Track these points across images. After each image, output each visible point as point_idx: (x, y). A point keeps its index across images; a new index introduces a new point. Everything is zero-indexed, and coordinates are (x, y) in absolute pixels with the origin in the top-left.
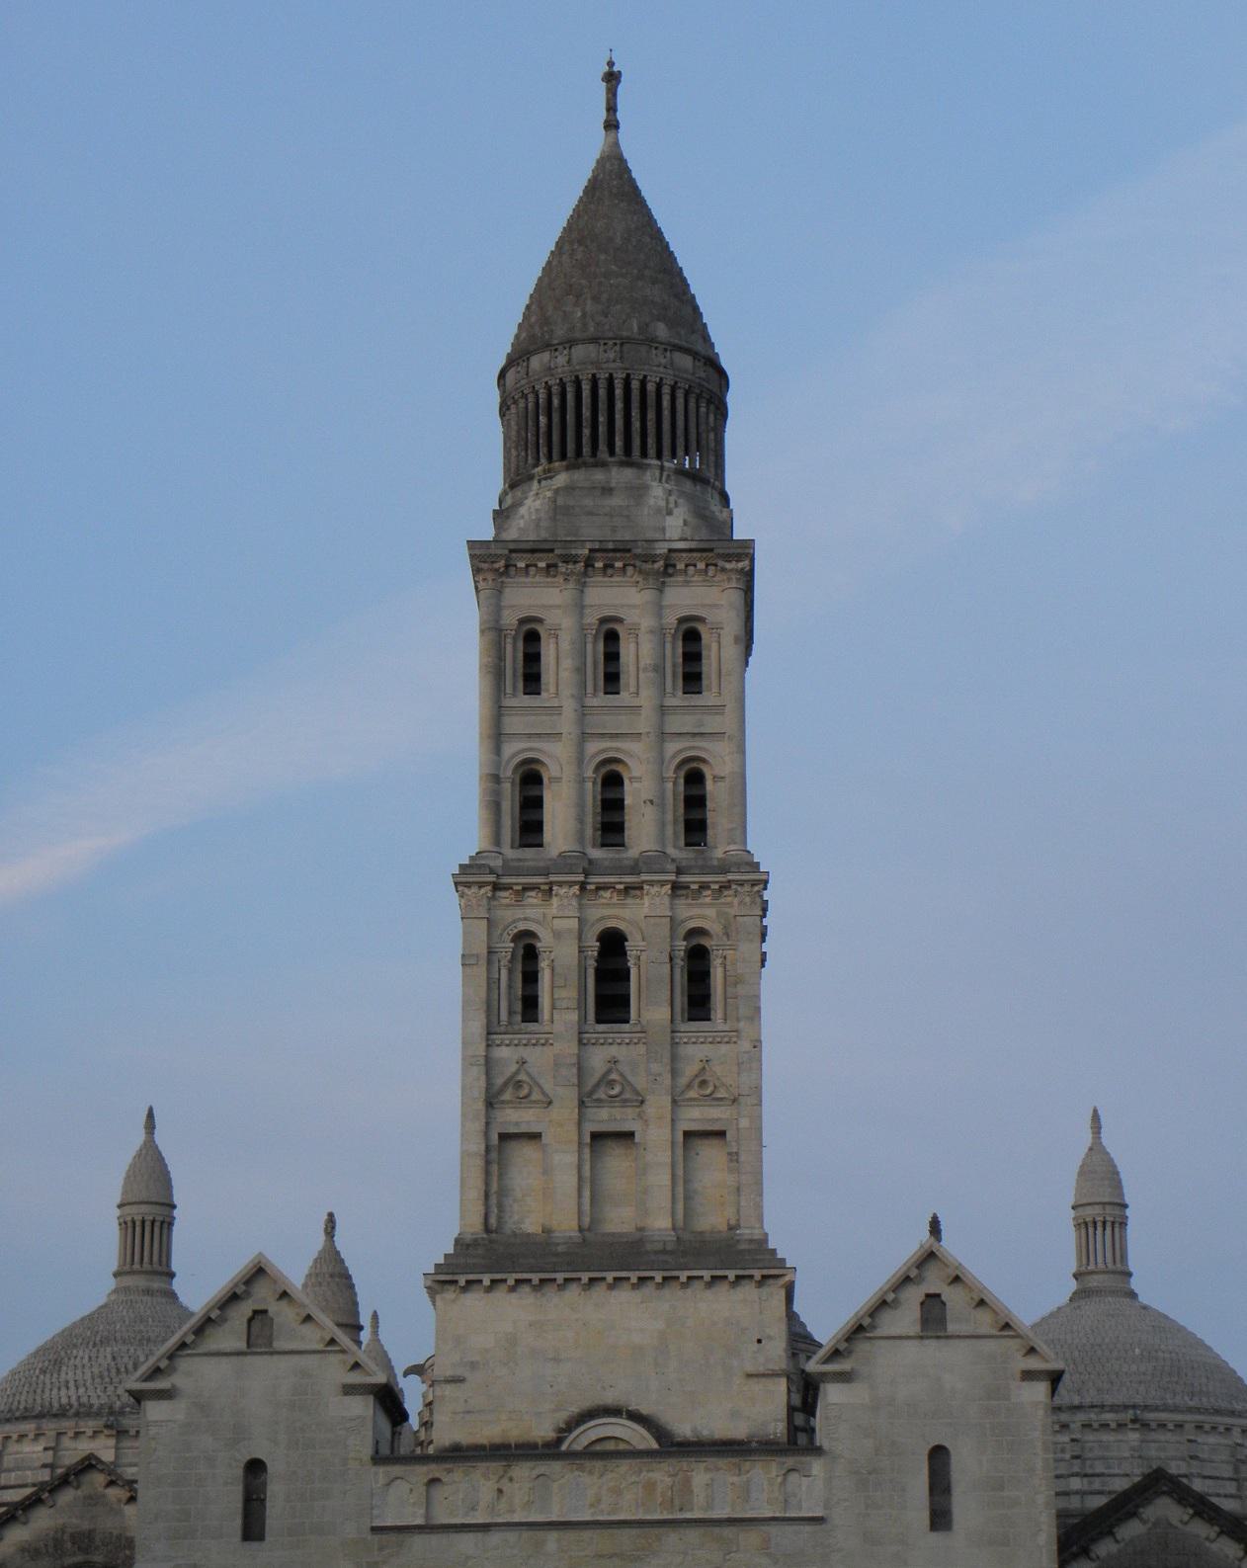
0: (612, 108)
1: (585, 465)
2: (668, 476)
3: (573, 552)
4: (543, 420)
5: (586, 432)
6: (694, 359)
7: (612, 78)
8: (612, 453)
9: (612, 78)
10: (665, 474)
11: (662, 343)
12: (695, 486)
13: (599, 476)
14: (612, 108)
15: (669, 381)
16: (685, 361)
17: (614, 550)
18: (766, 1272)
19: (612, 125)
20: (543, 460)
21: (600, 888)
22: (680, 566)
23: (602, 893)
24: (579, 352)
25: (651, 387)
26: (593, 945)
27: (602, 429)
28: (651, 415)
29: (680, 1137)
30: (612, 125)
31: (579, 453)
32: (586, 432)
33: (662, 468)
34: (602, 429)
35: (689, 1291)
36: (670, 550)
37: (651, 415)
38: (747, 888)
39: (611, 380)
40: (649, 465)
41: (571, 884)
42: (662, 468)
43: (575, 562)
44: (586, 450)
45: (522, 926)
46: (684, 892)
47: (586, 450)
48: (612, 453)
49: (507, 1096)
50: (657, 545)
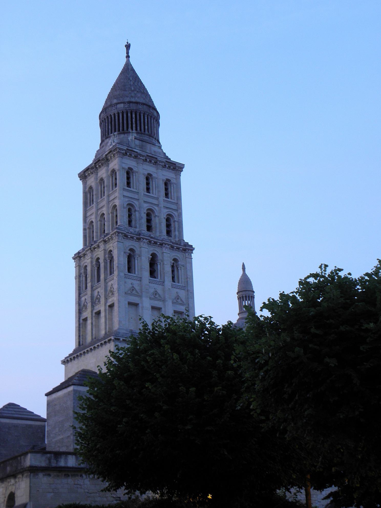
0: (128, 53)
2: (116, 136)
3: (92, 166)
6: (124, 104)
7: (128, 47)
9: (128, 47)
10: (115, 136)
11: (113, 104)
12: (125, 135)
14: (128, 53)
15: (116, 113)
16: (122, 105)
18: (108, 339)
19: (128, 57)
21: (95, 248)
22: (109, 158)
23: (96, 249)
25: (113, 116)
26: (94, 263)
29: (107, 307)
30: (128, 57)
33: (114, 135)
35: (99, 349)
36: (106, 155)
38: (114, 235)
40: (111, 135)
41: (88, 250)
42: (114, 135)
43: (94, 168)
45: (85, 265)
46: (107, 242)
49: (84, 309)
50: (103, 155)
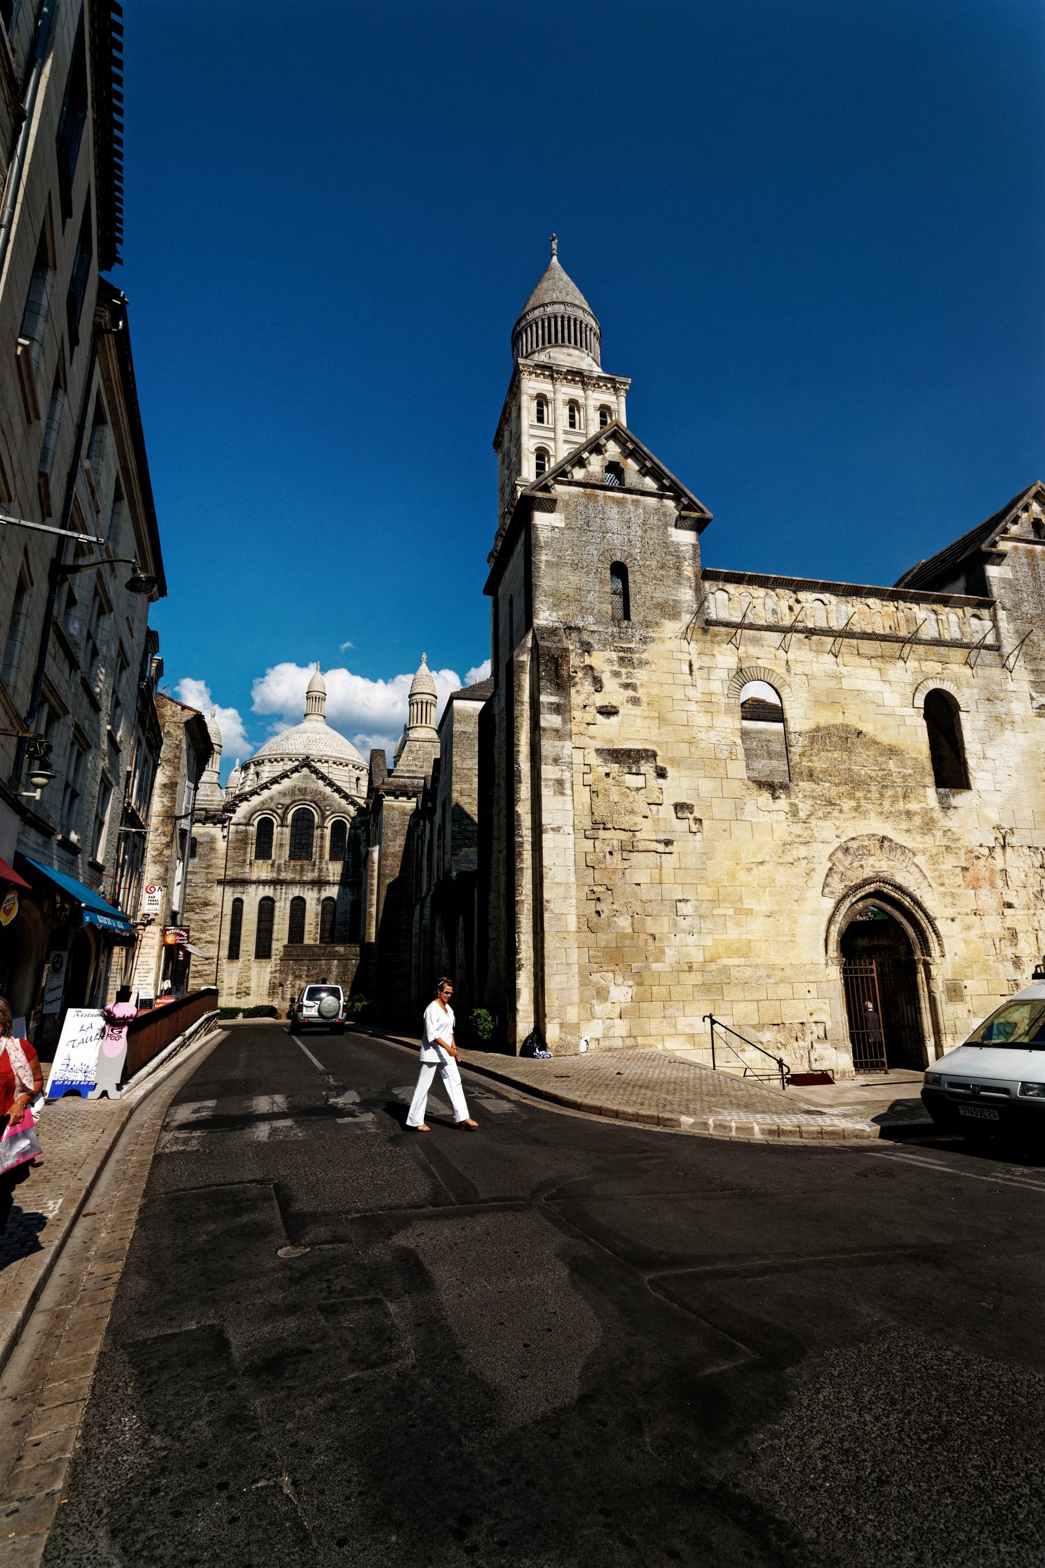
1: (560, 346)
4: (540, 332)
5: (560, 335)
8: (570, 342)
13: (565, 350)
17: (577, 373)
20: (540, 346)
24: (556, 306)
27: (566, 335)
28: (584, 335)
31: (556, 341)
32: (560, 335)
34: (566, 335)
37: (584, 335)
39: (569, 318)
44: (560, 341)
47: (560, 341)
48: (570, 342)
